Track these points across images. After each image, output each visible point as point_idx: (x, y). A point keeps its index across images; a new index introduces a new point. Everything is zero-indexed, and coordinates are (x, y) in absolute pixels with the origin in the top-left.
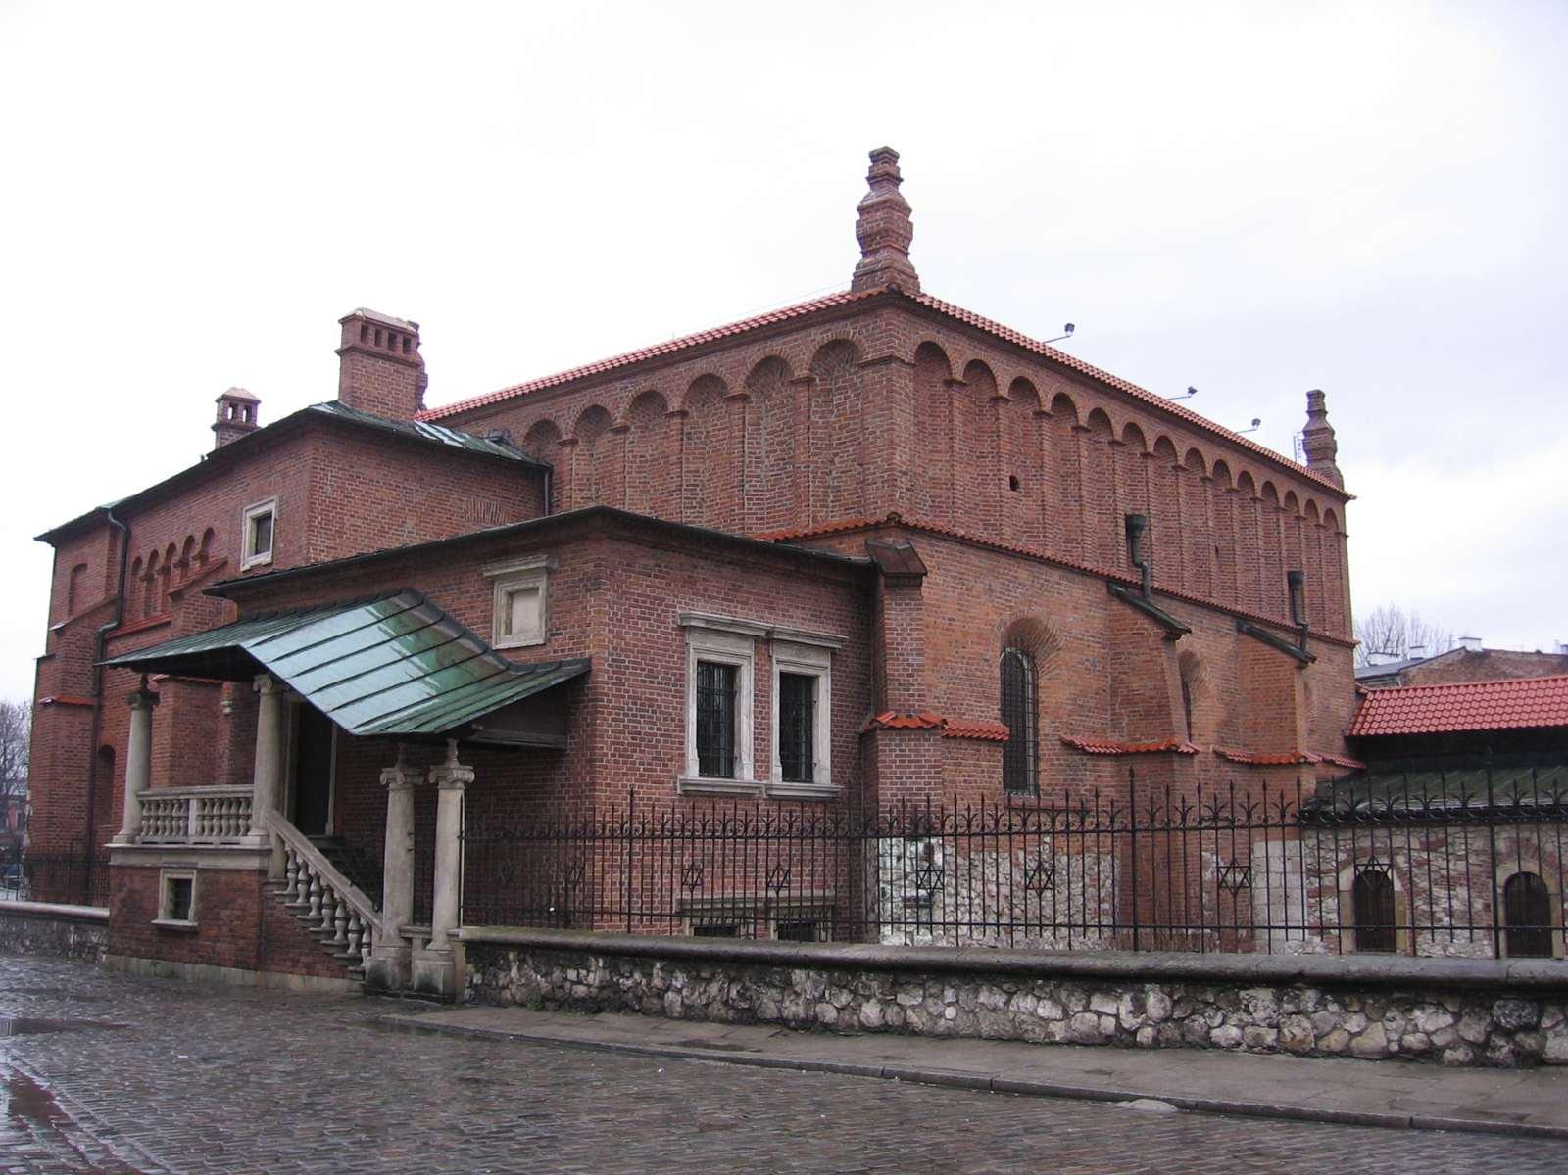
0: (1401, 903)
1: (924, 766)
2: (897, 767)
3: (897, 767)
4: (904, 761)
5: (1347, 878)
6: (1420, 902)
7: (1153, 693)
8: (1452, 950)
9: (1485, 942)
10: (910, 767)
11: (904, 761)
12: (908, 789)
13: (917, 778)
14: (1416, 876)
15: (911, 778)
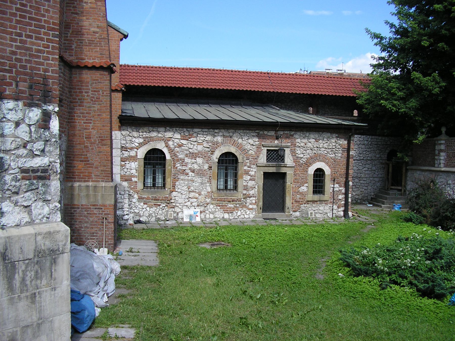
0: (170, 165)
1: (43, 27)
2: (18, 22)
3: (18, 22)
4: (24, 17)
5: (142, 153)
6: (179, 165)
7: (98, 30)
8: (192, 188)
9: (208, 185)
10: (30, 25)
11: (24, 17)
12: (28, 49)
13: (37, 38)
14: (178, 152)
15: (31, 37)
